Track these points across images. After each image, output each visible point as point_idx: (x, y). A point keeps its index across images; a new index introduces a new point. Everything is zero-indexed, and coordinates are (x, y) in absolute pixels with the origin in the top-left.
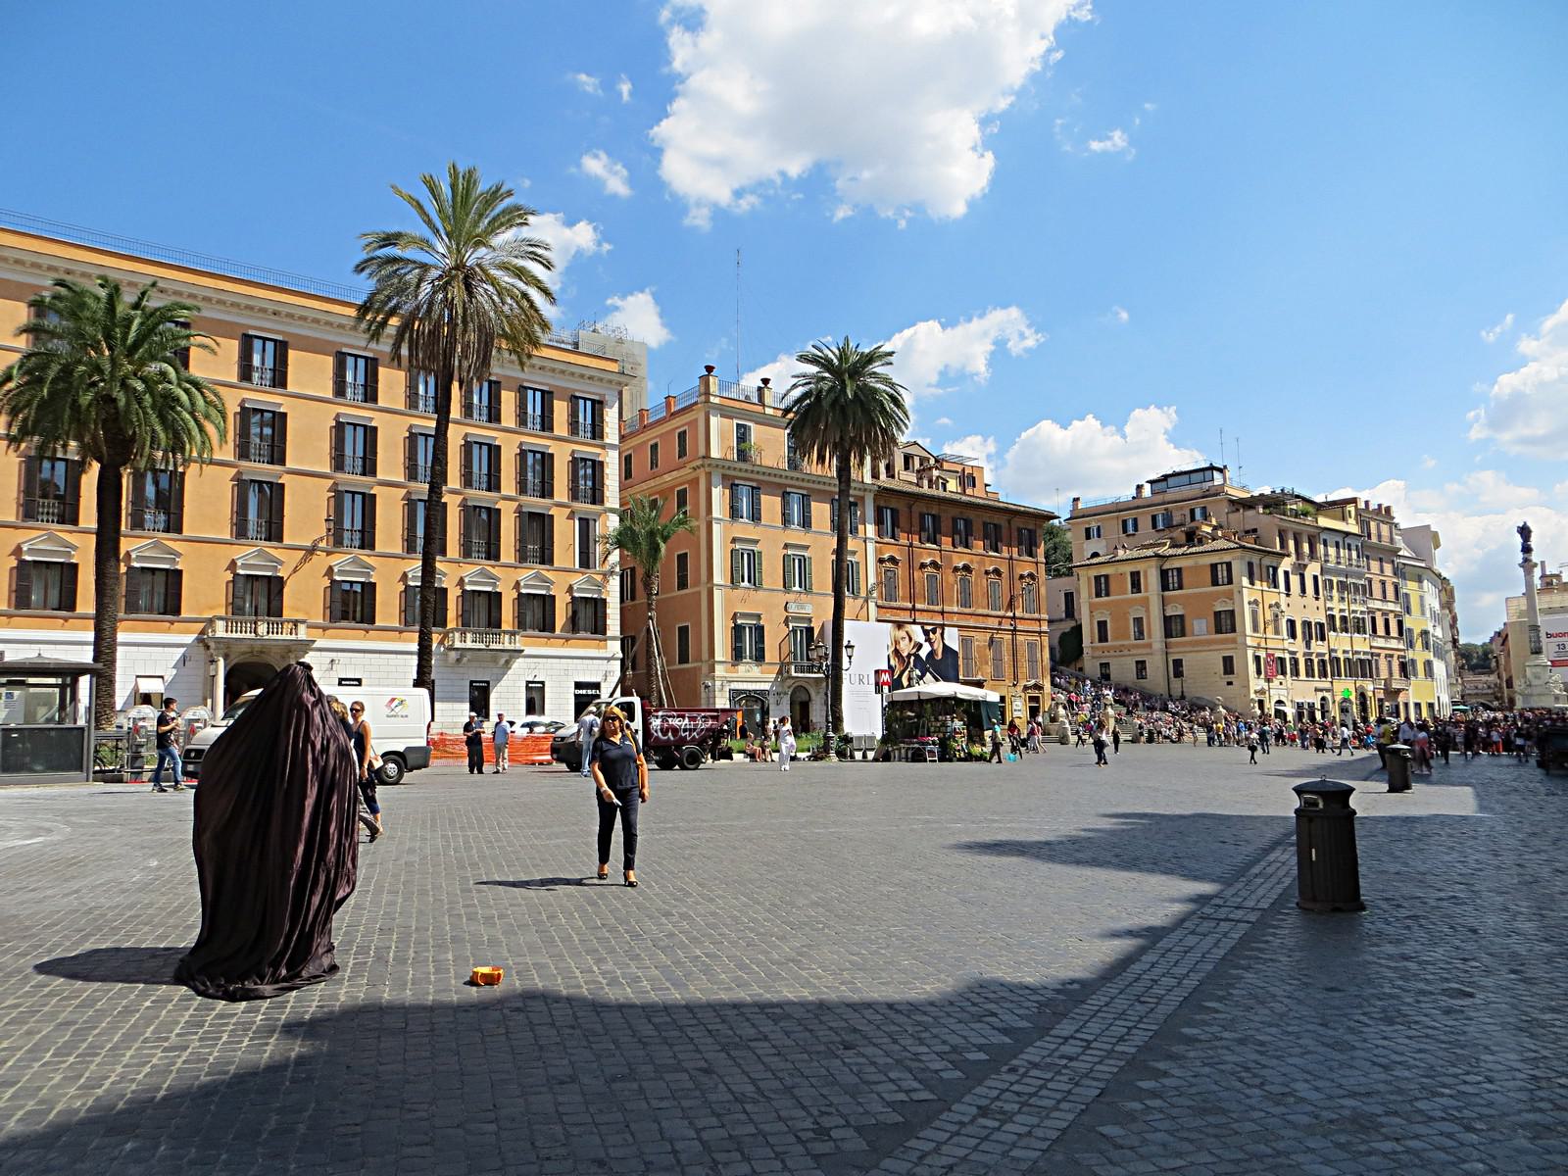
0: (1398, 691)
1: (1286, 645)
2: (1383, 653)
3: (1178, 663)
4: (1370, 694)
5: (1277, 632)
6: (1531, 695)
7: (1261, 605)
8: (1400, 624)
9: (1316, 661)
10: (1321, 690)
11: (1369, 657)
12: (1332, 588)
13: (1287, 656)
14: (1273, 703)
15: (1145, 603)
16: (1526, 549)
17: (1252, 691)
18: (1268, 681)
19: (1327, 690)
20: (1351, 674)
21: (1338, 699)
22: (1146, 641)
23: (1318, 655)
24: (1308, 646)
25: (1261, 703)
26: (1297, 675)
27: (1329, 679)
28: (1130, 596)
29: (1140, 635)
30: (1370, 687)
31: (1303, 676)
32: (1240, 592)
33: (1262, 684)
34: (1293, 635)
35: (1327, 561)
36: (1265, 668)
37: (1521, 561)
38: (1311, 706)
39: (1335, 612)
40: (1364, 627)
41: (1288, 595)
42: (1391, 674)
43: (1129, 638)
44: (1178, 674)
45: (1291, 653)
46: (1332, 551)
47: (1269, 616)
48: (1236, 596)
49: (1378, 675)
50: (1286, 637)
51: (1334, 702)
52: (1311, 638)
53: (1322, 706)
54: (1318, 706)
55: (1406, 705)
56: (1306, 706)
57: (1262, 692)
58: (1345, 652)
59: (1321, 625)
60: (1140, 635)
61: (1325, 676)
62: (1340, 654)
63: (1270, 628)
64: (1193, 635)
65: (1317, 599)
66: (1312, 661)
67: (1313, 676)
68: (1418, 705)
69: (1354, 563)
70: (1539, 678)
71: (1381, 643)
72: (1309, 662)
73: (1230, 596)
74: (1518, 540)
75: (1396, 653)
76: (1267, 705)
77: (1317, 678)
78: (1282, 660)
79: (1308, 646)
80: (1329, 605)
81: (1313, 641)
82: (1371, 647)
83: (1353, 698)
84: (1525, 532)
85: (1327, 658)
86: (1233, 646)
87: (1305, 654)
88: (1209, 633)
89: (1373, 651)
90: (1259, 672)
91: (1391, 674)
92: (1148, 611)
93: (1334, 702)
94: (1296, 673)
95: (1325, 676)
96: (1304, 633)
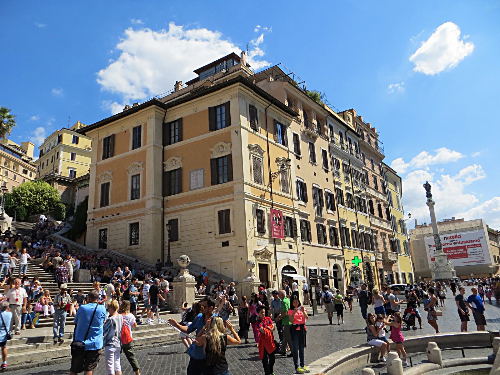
0: (393, 262)
1: (296, 204)
2: (380, 231)
3: (174, 223)
4: (373, 264)
5: (285, 189)
6: (439, 272)
7: (265, 154)
8: (388, 210)
9: (327, 228)
10: (334, 258)
11: (370, 233)
12: (338, 167)
13: (298, 218)
14: (280, 269)
15: (143, 156)
16: (429, 195)
17: (250, 253)
18: (274, 241)
19: (339, 258)
20: (357, 245)
21: (349, 267)
22: (141, 199)
23: (330, 222)
24: (319, 212)
25: (264, 268)
26: (309, 239)
27: (340, 248)
28: (131, 152)
29: (135, 194)
30: (373, 259)
31: (315, 241)
32: (238, 133)
33: (265, 244)
34: (304, 198)
35: (333, 142)
36: (270, 226)
37: (427, 201)
38: (325, 273)
39: (342, 188)
40: (365, 208)
41: (298, 158)
42: (385, 249)
43: (126, 199)
44: (174, 236)
45: (301, 214)
46: (337, 137)
47: (275, 168)
48: (234, 136)
49: (377, 249)
50: (295, 196)
51: (346, 270)
52: (322, 205)
53: (335, 273)
54: (331, 274)
55: (397, 274)
56: (319, 274)
57: (265, 254)
58: (352, 224)
59: (331, 196)
60: (135, 194)
61: (337, 244)
62: (347, 225)
63: (277, 182)
64: (190, 190)
65: (326, 171)
66: (323, 227)
67: (325, 243)
68: (404, 275)
69: (354, 153)
70: (442, 263)
71: (376, 222)
72: (321, 229)
73: (227, 139)
74: (424, 191)
75: (388, 233)
76: (272, 272)
77: (329, 246)
78: (292, 221)
79: (319, 212)
80: (336, 180)
81: (324, 209)
82: (371, 225)
83: (361, 267)
84: (427, 187)
85: (337, 226)
86: (229, 197)
87: (316, 220)
88: (205, 185)
89: (373, 228)
90: (261, 230)
91: (385, 249)
92: (144, 165)
93: (346, 270)
94: (307, 236)
95: (337, 244)
96: (315, 198)
